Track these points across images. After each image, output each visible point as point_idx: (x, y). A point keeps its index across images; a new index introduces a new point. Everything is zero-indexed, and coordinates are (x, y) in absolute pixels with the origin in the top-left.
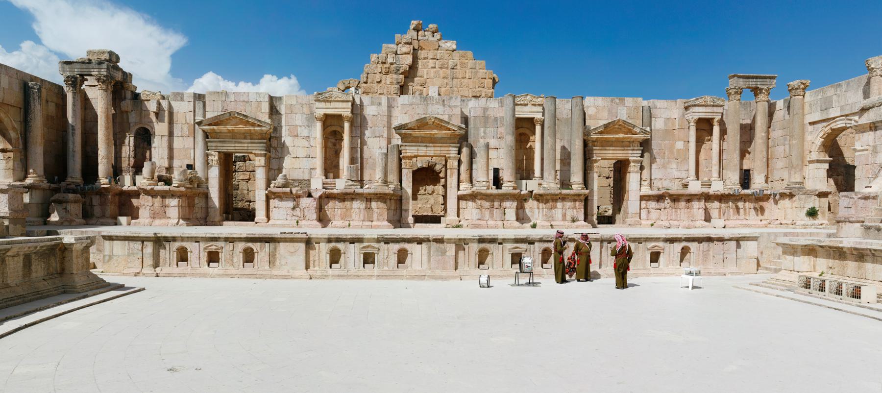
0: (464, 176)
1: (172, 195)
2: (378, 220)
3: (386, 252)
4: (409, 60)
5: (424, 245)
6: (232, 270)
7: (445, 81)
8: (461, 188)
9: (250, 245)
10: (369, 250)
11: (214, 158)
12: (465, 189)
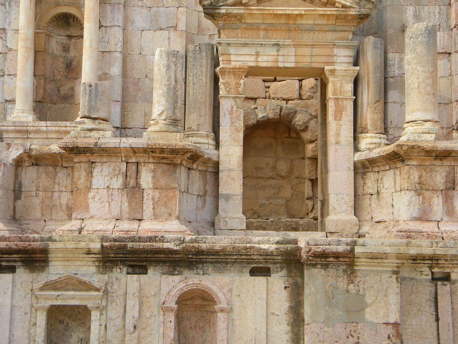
0: (369, 116)
2: (156, 217)
3: (133, 304)
8: (364, 143)
10: (72, 298)
12: (372, 144)
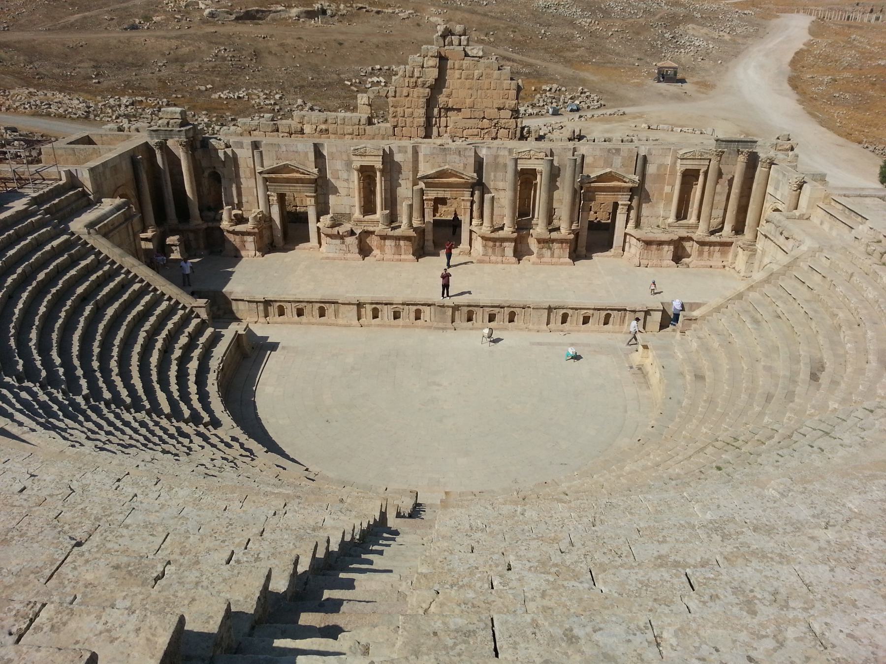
0: (476, 213)
1: (248, 234)
4: (435, 73)
5: (432, 307)
6: (314, 320)
7: (470, 91)
9: (322, 305)
11: (274, 198)
